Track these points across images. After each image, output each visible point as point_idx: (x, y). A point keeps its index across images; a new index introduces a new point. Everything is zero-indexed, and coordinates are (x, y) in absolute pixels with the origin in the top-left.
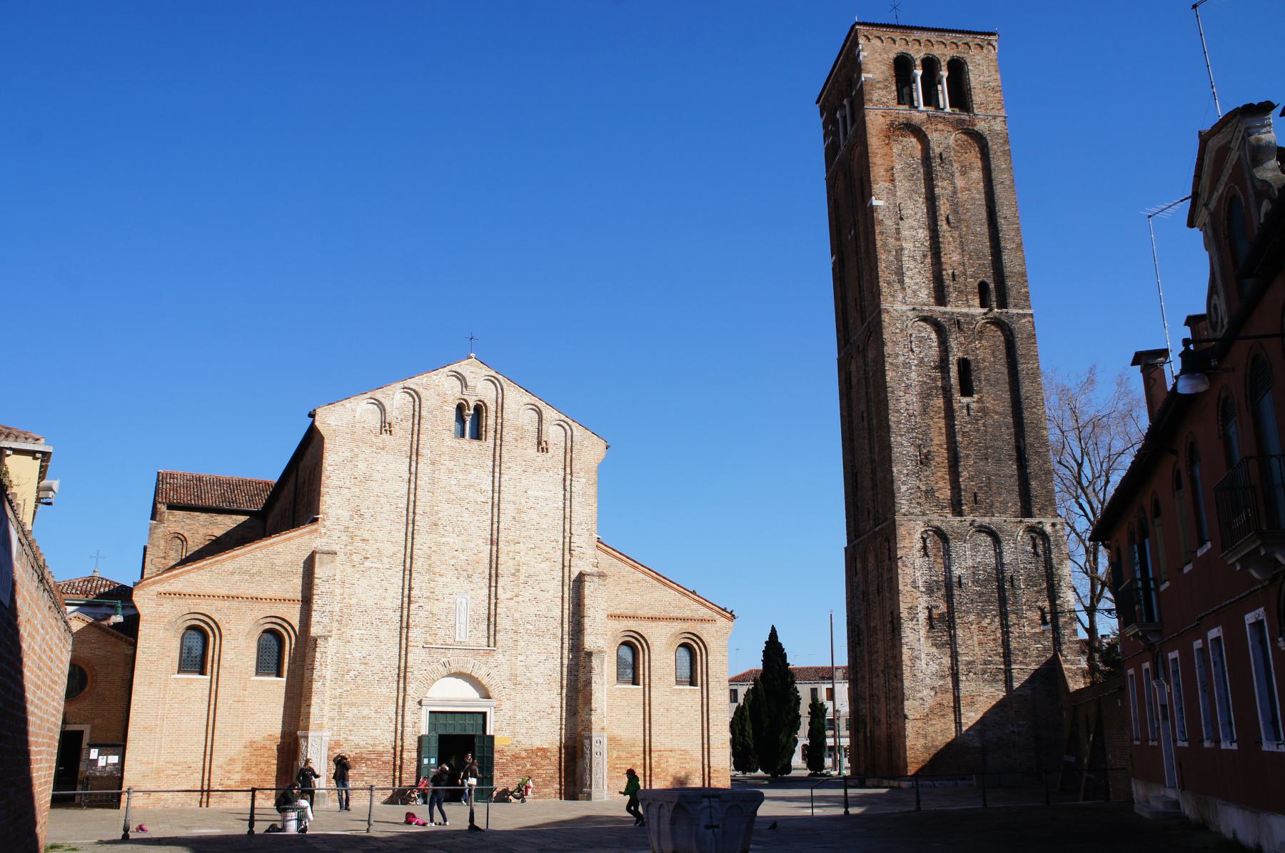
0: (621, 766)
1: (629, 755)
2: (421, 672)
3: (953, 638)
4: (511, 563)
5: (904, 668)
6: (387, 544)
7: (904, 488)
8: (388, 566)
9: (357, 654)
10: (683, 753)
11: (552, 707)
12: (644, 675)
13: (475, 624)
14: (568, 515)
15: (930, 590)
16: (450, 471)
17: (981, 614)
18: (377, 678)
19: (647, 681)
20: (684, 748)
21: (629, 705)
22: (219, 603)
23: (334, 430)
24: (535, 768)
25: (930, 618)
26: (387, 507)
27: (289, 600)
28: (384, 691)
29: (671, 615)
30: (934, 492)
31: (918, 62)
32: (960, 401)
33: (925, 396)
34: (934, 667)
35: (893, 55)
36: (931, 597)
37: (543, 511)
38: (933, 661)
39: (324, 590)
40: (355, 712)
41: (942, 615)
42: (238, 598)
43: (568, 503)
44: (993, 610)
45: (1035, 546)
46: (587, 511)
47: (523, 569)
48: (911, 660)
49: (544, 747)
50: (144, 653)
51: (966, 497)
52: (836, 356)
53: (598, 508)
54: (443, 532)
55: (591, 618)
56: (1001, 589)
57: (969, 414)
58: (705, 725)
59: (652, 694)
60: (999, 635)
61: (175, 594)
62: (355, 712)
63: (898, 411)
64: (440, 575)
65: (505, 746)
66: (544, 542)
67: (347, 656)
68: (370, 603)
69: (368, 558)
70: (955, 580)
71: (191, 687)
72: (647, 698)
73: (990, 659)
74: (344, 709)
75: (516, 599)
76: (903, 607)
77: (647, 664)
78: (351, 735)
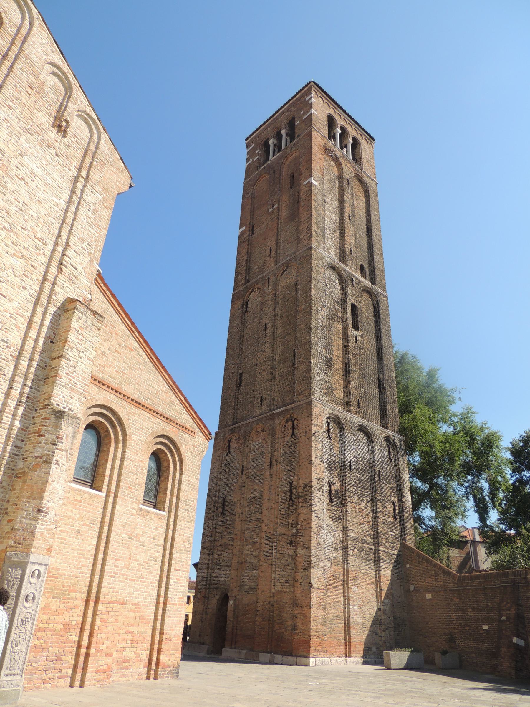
3: (344, 513)
5: (312, 535)
7: (317, 378)
12: (111, 477)
14: (69, 220)
15: (330, 468)
17: (361, 497)
19: (113, 487)
20: (136, 601)
25: (330, 492)
29: (157, 407)
30: (332, 389)
31: (339, 126)
32: (352, 332)
33: (331, 317)
34: (330, 539)
35: (327, 112)
36: (330, 473)
38: (330, 532)
41: (337, 491)
43: (73, 208)
44: (367, 496)
45: (389, 453)
46: (94, 232)
48: (317, 528)
51: (353, 401)
52: (231, 291)
53: (108, 236)
55: (71, 363)
56: (372, 478)
57: (356, 342)
58: (166, 568)
59: (118, 507)
60: (370, 518)
63: (317, 320)
66: (26, 232)
70: (348, 463)
72: (108, 513)
73: (365, 538)
76: (314, 477)
77: (118, 462)
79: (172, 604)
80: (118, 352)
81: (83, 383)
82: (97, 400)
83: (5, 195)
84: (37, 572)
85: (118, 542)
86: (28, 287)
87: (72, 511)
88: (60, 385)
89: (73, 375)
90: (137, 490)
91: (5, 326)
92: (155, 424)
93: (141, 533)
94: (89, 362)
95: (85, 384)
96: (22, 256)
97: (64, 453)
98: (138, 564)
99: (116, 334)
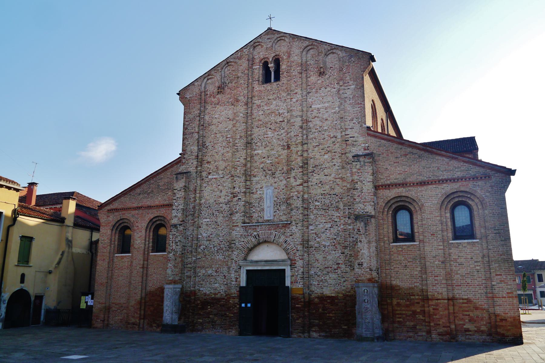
0: (401, 312)
1: (408, 303)
2: (240, 243)
4: (299, 159)
6: (221, 162)
8: (222, 176)
9: (205, 235)
10: (465, 301)
11: (337, 264)
13: (278, 206)
16: (259, 106)
18: (216, 249)
20: (466, 297)
21: (406, 259)
22: (133, 212)
23: (189, 100)
24: (326, 312)
26: (221, 139)
27: (166, 205)
28: (221, 257)
37: (324, 117)
39: (179, 196)
40: (204, 272)
42: (142, 207)
46: (356, 109)
47: (311, 162)
49: (333, 295)
50: (102, 243)
54: (255, 148)
61: (114, 210)
62: (204, 272)
64: (254, 176)
65: (300, 294)
67: (199, 236)
68: (212, 201)
69: (211, 173)
71: (123, 260)
74: (198, 270)
75: (305, 185)
78: (202, 287)
79: (500, 297)
80: (396, 162)
81: (369, 196)
82: (390, 197)
83: (311, 132)
84: (366, 291)
85: (434, 267)
86: (336, 163)
87: (398, 257)
88: (356, 203)
89: (362, 195)
90: (439, 234)
91: (332, 188)
92: (443, 189)
93: (457, 257)
94: (369, 183)
95: (371, 196)
96: (328, 152)
97: (363, 236)
98: (460, 276)
99: (391, 153)
